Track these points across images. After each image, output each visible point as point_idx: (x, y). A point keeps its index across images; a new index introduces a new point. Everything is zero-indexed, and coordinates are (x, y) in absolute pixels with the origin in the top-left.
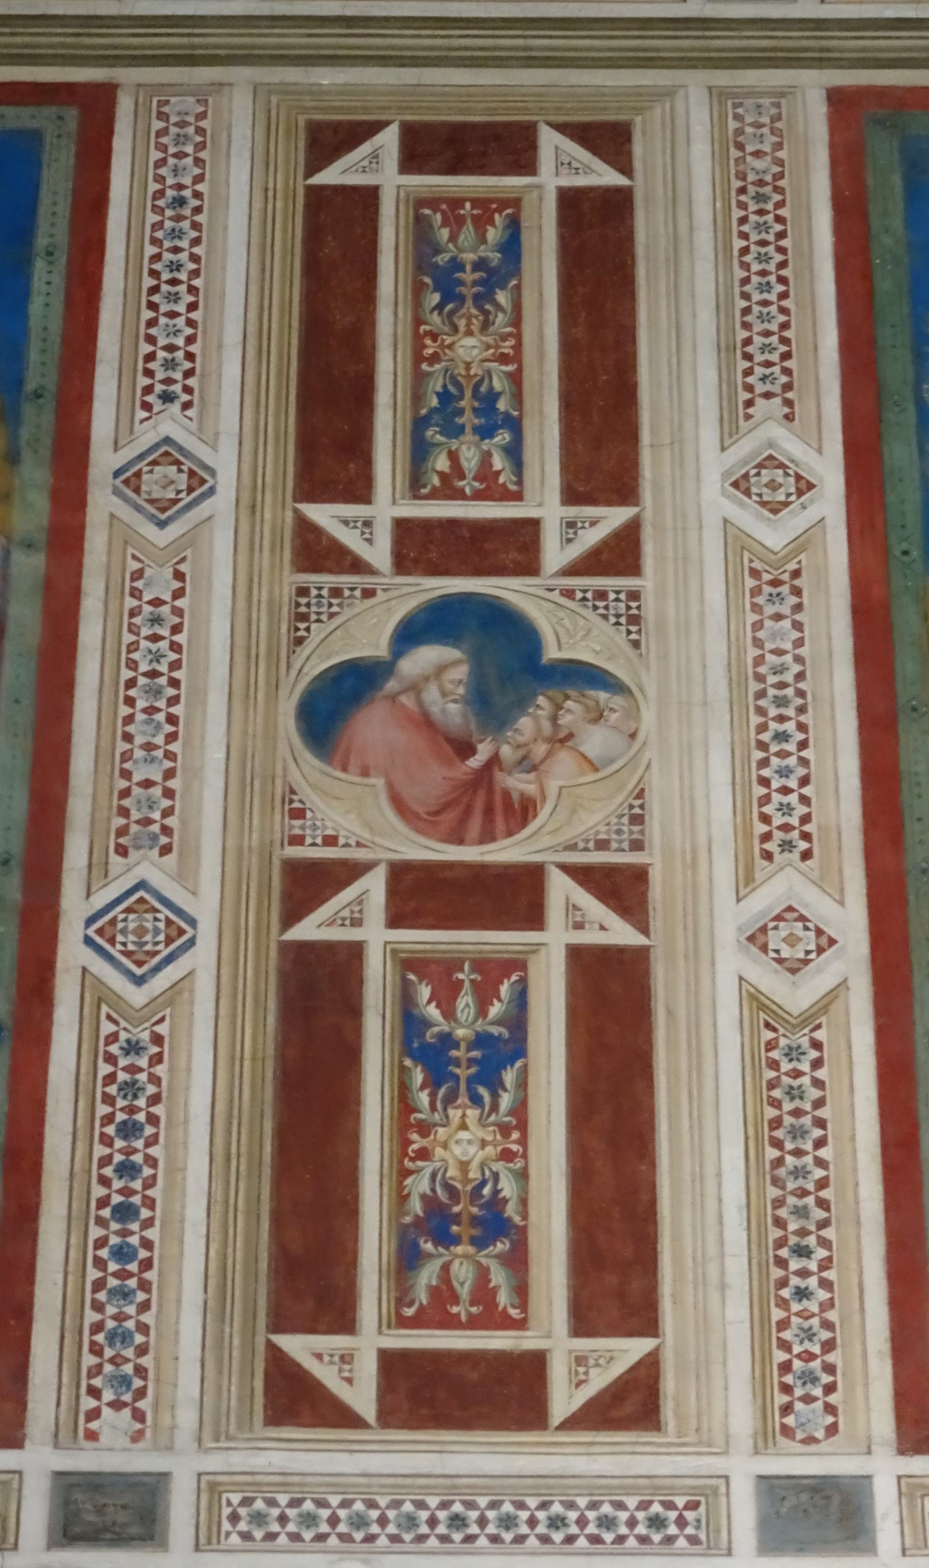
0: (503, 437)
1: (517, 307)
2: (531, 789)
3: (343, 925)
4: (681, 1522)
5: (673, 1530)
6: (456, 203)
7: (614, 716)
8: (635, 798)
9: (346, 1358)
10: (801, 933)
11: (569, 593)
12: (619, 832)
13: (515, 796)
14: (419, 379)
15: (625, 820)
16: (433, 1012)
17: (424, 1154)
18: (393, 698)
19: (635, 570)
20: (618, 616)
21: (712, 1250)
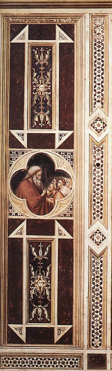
0: (48, 112)
1: (51, 76)
2: (52, 202)
3: (19, 234)
4: (75, 363)
5: (74, 364)
6: (40, 47)
7: (68, 184)
8: (71, 204)
9: (21, 329)
10: (100, 236)
11: (60, 153)
12: (68, 212)
13: (50, 203)
14: (32, 96)
15: (69, 209)
16: (35, 254)
17: (33, 285)
18: (27, 179)
19: (73, 148)
20: (69, 159)
21: (82, 307)
